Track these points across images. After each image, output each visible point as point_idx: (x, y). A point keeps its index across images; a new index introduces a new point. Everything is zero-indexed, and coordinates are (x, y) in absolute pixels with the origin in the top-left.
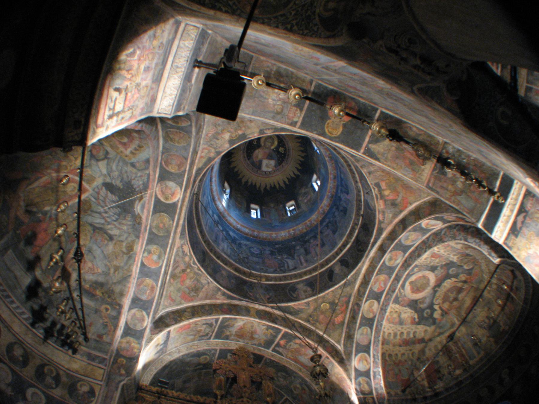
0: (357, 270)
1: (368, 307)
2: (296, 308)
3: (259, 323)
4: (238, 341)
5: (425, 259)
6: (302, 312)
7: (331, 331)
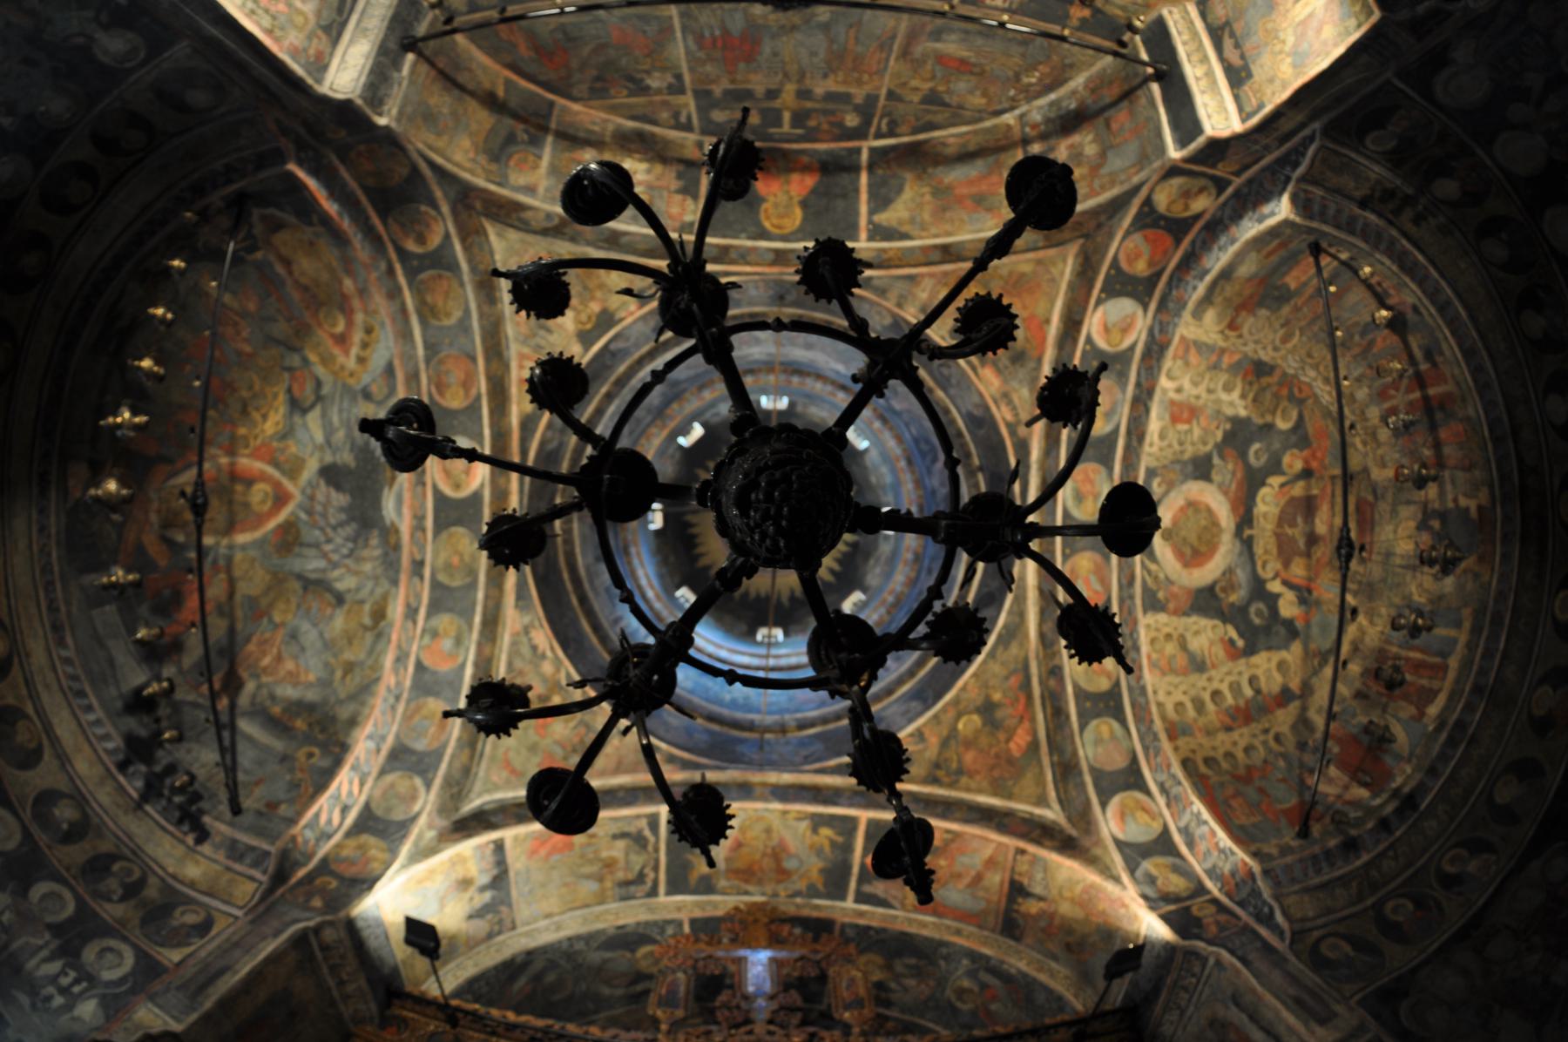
4: (746, 893)
7: (1010, 783)
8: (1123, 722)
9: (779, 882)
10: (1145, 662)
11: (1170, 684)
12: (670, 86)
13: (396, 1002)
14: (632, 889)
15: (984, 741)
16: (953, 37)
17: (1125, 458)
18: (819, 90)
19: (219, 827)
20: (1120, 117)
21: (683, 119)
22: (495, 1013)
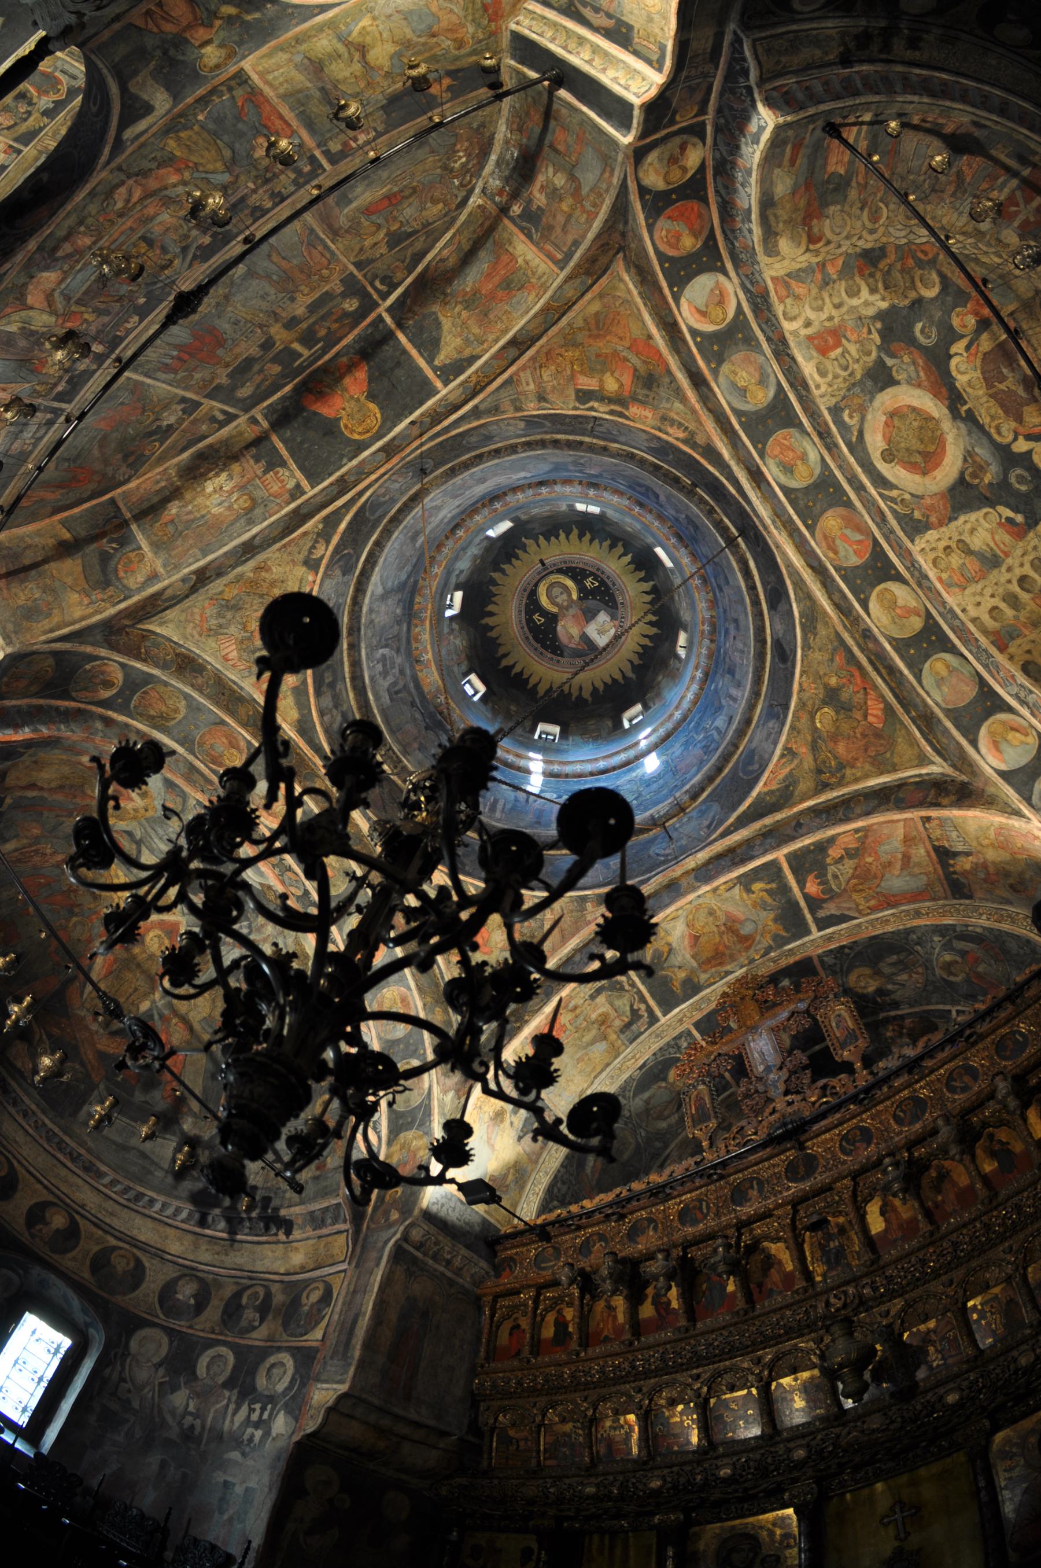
0: (790, 575)
2: (774, 787)
4: (728, 973)
8: (954, 650)
9: (748, 948)
10: (938, 586)
11: (974, 594)
12: (184, 411)
13: (498, 1248)
14: (634, 1027)
16: (359, 190)
17: (805, 409)
18: (300, 311)
19: (294, 1211)
20: (558, 136)
21: (221, 417)
22: (574, 1208)
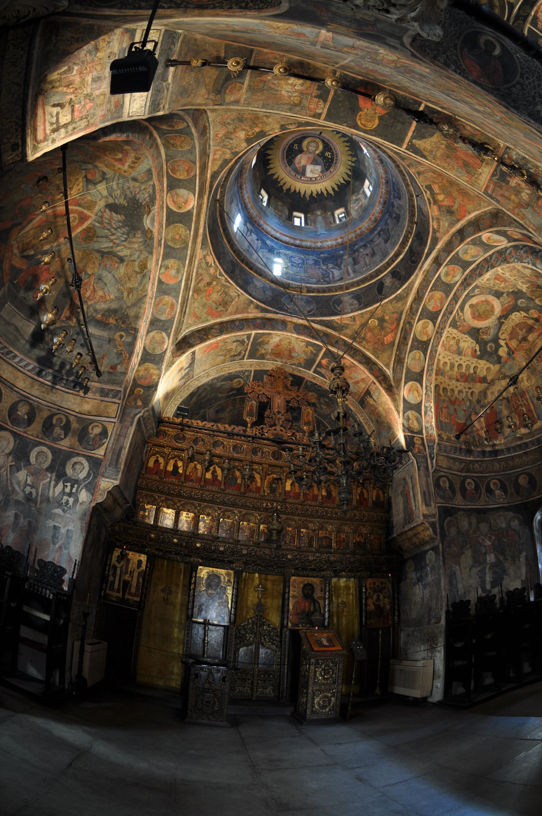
1: (421, 328)
3: (298, 338)
5: (488, 280)
6: (347, 328)
15: (376, 331)
